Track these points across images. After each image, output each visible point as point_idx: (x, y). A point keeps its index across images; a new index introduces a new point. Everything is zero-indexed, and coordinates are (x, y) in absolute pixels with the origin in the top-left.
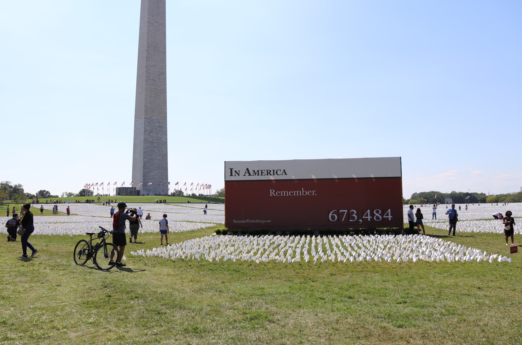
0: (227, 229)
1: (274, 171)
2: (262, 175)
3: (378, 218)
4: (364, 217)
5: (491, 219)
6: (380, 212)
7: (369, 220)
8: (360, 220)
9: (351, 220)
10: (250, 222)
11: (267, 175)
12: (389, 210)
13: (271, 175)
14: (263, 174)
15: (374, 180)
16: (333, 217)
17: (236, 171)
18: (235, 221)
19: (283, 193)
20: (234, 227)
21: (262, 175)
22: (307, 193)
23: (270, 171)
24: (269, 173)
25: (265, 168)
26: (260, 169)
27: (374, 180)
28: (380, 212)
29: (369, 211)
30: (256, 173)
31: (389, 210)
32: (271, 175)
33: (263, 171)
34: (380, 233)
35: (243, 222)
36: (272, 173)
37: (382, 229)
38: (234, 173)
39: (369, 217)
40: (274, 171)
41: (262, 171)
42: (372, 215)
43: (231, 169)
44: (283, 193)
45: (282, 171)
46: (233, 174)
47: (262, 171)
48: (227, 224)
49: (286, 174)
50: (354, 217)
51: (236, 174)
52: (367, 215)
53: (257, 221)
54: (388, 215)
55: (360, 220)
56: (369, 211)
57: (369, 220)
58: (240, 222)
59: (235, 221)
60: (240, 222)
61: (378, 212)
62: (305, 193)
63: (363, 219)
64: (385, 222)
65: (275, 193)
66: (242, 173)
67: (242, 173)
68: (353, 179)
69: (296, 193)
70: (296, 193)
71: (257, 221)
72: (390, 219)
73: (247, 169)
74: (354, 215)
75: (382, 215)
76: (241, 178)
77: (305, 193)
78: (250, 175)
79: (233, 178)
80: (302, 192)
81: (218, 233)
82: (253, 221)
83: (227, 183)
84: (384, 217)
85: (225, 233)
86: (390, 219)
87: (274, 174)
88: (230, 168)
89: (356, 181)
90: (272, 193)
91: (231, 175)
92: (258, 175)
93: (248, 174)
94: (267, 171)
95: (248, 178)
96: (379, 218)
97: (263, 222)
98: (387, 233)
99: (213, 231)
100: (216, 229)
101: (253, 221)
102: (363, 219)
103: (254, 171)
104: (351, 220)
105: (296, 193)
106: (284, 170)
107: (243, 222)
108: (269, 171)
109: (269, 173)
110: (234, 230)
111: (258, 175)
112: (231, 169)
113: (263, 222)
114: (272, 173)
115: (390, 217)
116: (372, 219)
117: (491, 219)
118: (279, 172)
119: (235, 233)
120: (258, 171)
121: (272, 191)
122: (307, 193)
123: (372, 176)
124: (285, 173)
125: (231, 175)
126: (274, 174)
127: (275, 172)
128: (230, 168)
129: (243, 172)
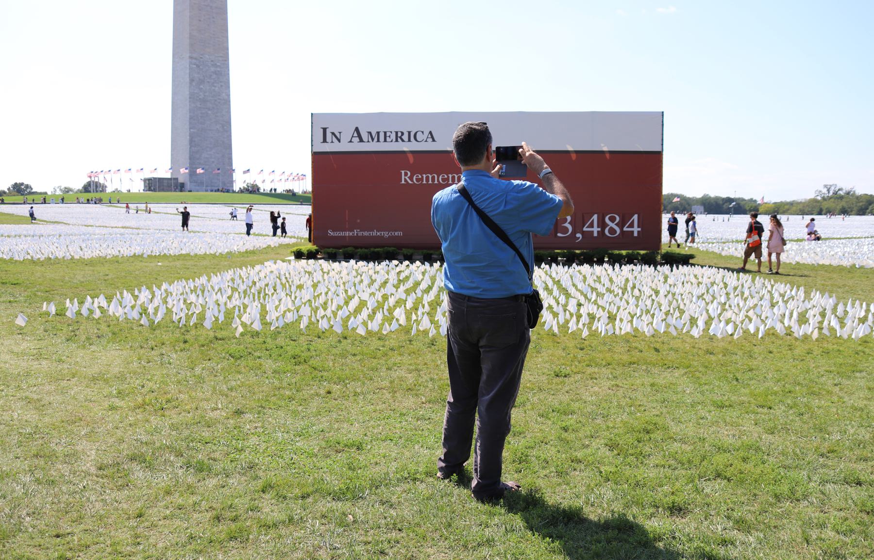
1: (409, 133)
2: (385, 141)
3: (612, 231)
4: (585, 229)
5: (802, 240)
6: (618, 219)
7: (595, 234)
8: (579, 235)
9: (559, 235)
10: (360, 234)
11: (397, 141)
12: (636, 217)
13: (403, 141)
14: (388, 139)
15: (608, 156)
17: (333, 134)
18: (331, 233)
19: (427, 178)
21: (385, 141)
23: (403, 134)
24: (399, 137)
26: (382, 130)
27: (608, 156)
28: (618, 219)
29: (595, 217)
31: (636, 217)
32: (403, 141)
33: (388, 134)
34: (615, 260)
35: (347, 234)
36: (405, 137)
37: (616, 252)
38: (329, 135)
39: (596, 230)
40: (409, 133)
41: (385, 133)
42: (602, 224)
43: (325, 130)
44: (427, 178)
45: (426, 133)
47: (385, 133)
49: (434, 140)
50: (567, 229)
51: (334, 139)
52: (592, 225)
54: (632, 225)
55: (579, 235)
56: (595, 217)
57: (595, 234)
58: (342, 234)
59: (331, 233)
60: (342, 234)
61: (612, 219)
63: (583, 233)
64: (626, 240)
65: (411, 178)
67: (345, 138)
68: (567, 152)
71: (375, 233)
72: (636, 234)
73: (357, 129)
74: (567, 225)
75: (621, 225)
76: (344, 146)
78: (361, 140)
81: (299, 255)
82: (366, 234)
84: (625, 229)
85: (311, 255)
86: (636, 234)
87: (409, 140)
88: (323, 127)
89: (574, 157)
90: (405, 177)
91: (325, 141)
92: (378, 141)
94: (397, 133)
95: (357, 147)
97: (386, 234)
98: (631, 260)
99: (289, 251)
100: (295, 249)
101: (366, 234)
102: (583, 233)
103: (370, 133)
104: (559, 235)
106: (430, 133)
107: (347, 234)
108: (399, 134)
109: (399, 137)
110: (330, 250)
111: (378, 141)
112: (325, 130)
114: (405, 137)
115: (636, 230)
116: (601, 233)
117: (802, 240)
119: (332, 257)
120: (378, 133)
121: (406, 174)
123: (605, 149)
125: (325, 141)
126: (409, 140)
127: (413, 136)
128: (323, 127)
129: (347, 133)
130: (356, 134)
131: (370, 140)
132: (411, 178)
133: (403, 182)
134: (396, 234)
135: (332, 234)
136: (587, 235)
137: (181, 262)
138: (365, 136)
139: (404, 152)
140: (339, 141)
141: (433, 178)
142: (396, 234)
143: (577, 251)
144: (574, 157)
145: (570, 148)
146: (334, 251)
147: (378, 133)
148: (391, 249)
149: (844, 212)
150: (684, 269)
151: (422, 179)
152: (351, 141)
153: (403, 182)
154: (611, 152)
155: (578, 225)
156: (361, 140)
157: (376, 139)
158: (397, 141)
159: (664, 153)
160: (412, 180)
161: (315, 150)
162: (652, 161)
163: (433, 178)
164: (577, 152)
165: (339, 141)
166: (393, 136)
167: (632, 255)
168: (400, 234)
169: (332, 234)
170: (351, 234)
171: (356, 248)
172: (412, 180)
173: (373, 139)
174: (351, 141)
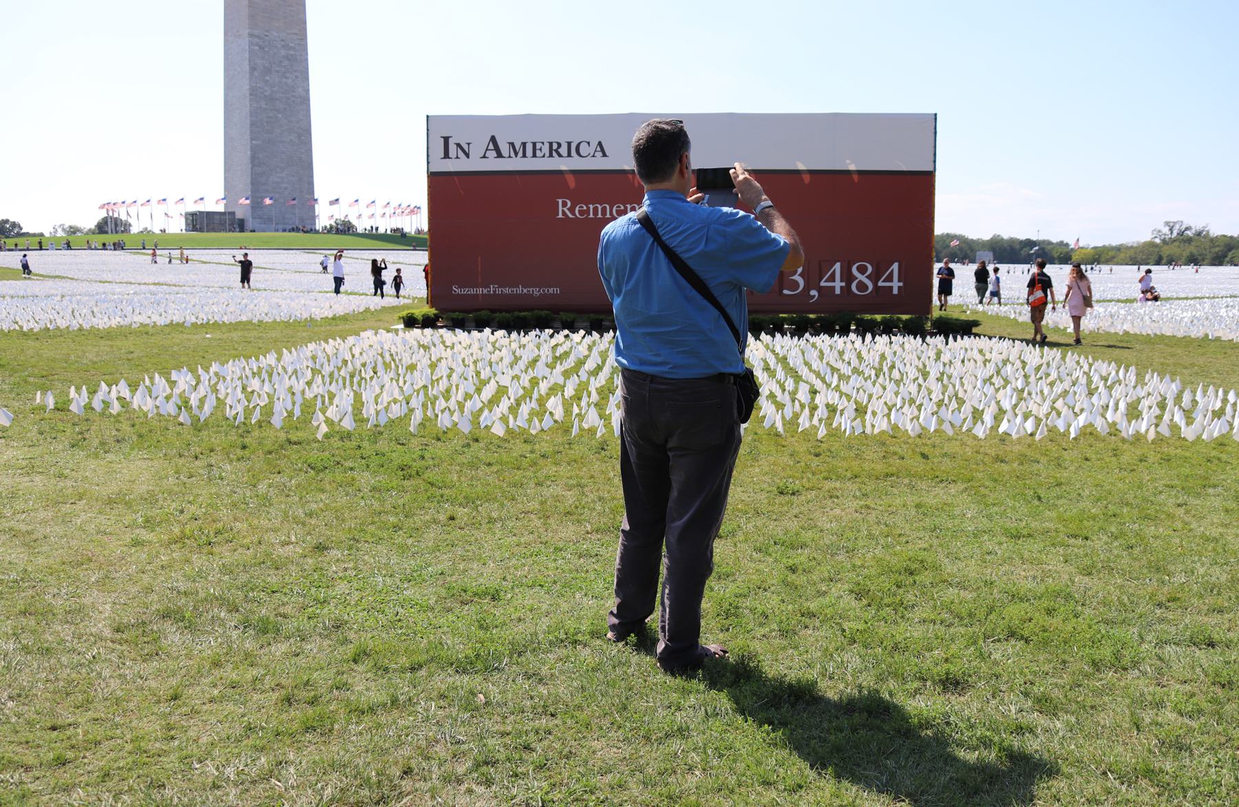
0: (433, 311)
1: (569, 144)
2: (534, 155)
3: (862, 286)
4: (823, 284)
7: (838, 291)
8: (813, 292)
9: (786, 292)
10: (499, 291)
11: (551, 155)
12: (895, 266)
13: (560, 155)
14: (538, 153)
15: (855, 177)
17: (458, 145)
18: (456, 290)
19: (596, 210)
20: (452, 308)
21: (534, 155)
23: (559, 145)
24: (554, 150)
25: (544, 136)
26: (529, 140)
27: (855, 177)
29: (837, 266)
31: (895, 266)
32: (560, 155)
33: (538, 146)
34: (866, 328)
35: (480, 291)
36: (563, 150)
37: (868, 317)
38: (453, 150)
39: (838, 285)
40: (569, 144)
41: (534, 144)
42: (848, 277)
43: (446, 140)
44: (596, 210)
45: (594, 144)
47: (534, 144)
48: (433, 299)
49: (604, 155)
50: (796, 284)
51: (461, 154)
52: (832, 278)
54: (890, 279)
55: (813, 292)
56: (837, 266)
57: (838, 291)
59: (456, 290)
60: (472, 291)
61: (862, 270)
63: (820, 289)
64: (882, 299)
65: (572, 210)
66: (477, 151)
67: (477, 151)
68: (797, 172)
71: (520, 290)
72: (895, 291)
73: (493, 139)
74: (797, 278)
75: (875, 277)
78: (500, 155)
81: (410, 322)
82: (507, 291)
83: (437, 181)
84: (880, 284)
86: (895, 291)
87: (569, 155)
88: (443, 136)
89: (807, 178)
90: (563, 209)
91: (446, 156)
92: (524, 156)
93: (494, 153)
94: (551, 144)
96: (867, 288)
97: (536, 292)
98: (888, 329)
99: (396, 316)
100: (404, 313)
101: (507, 291)
102: (820, 289)
103: (512, 144)
104: (786, 292)
106: (600, 144)
107: (480, 291)
108: (555, 146)
109: (554, 150)
110: (455, 315)
111: (524, 156)
112: (446, 140)
114: (563, 150)
115: (896, 285)
116: (847, 289)
118: (584, 149)
120: (524, 144)
121: (564, 204)
123: (852, 167)
124: (603, 150)
125: (446, 156)
126: (569, 155)
127: (575, 149)
128: (443, 136)
129: (479, 146)
130: (491, 147)
131: (512, 154)
132: (572, 210)
133: (560, 216)
134: (551, 291)
135: (458, 291)
136: (826, 293)
137: (240, 334)
138: (505, 150)
139: (561, 172)
142: (551, 291)
143: (812, 316)
144: (807, 178)
145: (801, 167)
146: (461, 316)
147: (524, 144)
148: (544, 313)
149: (1194, 260)
150: (966, 341)
151: (588, 211)
152: (484, 157)
153: (560, 216)
154: (860, 172)
155: (812, 278)
156: (500, 155)
157: (520, 154)
158: (551, 155)
159: (937, 174)
160: (573, 213)
161: (432, 170)
162: (918, 188)
163: (604, 210)
164: (811, 172)
167: (890, 320)
168: (557, 290)
169: (458, 291)
170: (485, 291)
171: (493, 311)
172: (573, 213)
173: (516, 154)
174: (484, 157)
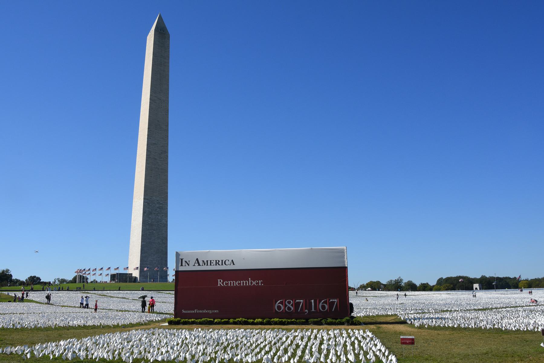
10: (198, 312)
14: (212, 264)
16: (279, 308)
17: (186, 262)
19: (231, 283)
22: (254, 283)
23: (219, 261)
24: (217, 263)
25: (214, 258)
26: (209, 260)
30: (205, 263)
36: (220, 263)
38: (184, 263)
45: (230, 261)
46: (184, 264)
48: (176, 315)
53: (205, 311)
58: (189, 312)
60: (189, 312)
62: (252, 283)
65: (223, 283)
67: (191, 264)
69: (243, 283)
70: (243, 283)
71: (205, 311)
73: (197, 260)
77: (252, 283)
78: (199, 265)
79: (181, 269)
80: (250, 282)
82: (201, 311)
90: (220, 283)
91: (182, 265)
97: (210, 312)
101: (201, 311)
103: (203, 261)
105: (243, 283)
112: (182, 260)
113: (210, 312)
114: (220, 263)
120: (207, 261)
121: (220, 281)
122: (254, 283)
124: (233, 263)
125: (182, 265)
132: (223, 283)
138: (201, 263)
140: (189, 265)
141: (233, 283)
147: (207, 261)
156: (199, 265)
160: (223, 284)
162: (341, 272)
163: (233, 283)
165: (189, 265)
166: (214, 263)
168: (217, 311)
172: (223, 284)
